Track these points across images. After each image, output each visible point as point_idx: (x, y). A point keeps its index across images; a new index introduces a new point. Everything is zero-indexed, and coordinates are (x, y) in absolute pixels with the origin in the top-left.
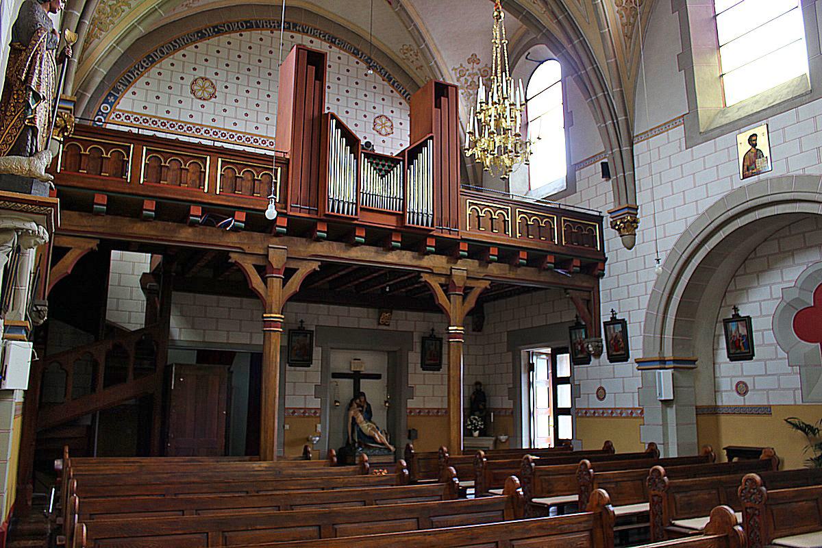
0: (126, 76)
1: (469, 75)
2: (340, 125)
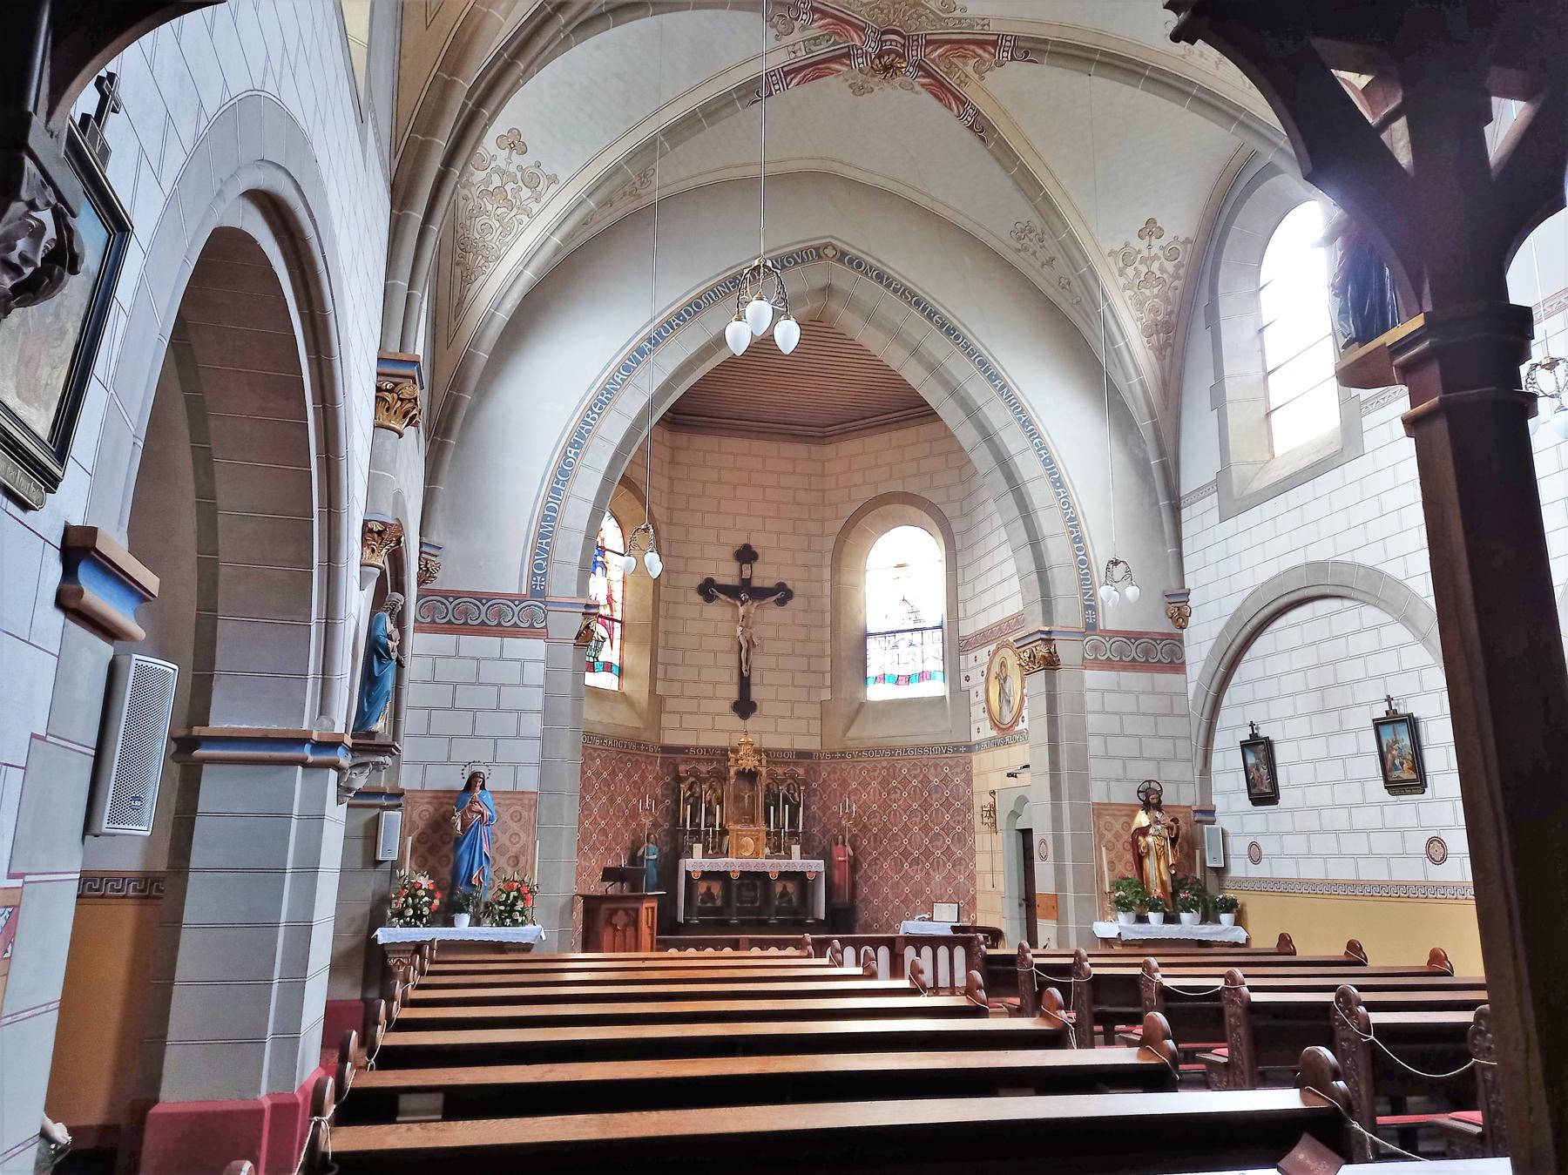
1: (1143, 261)
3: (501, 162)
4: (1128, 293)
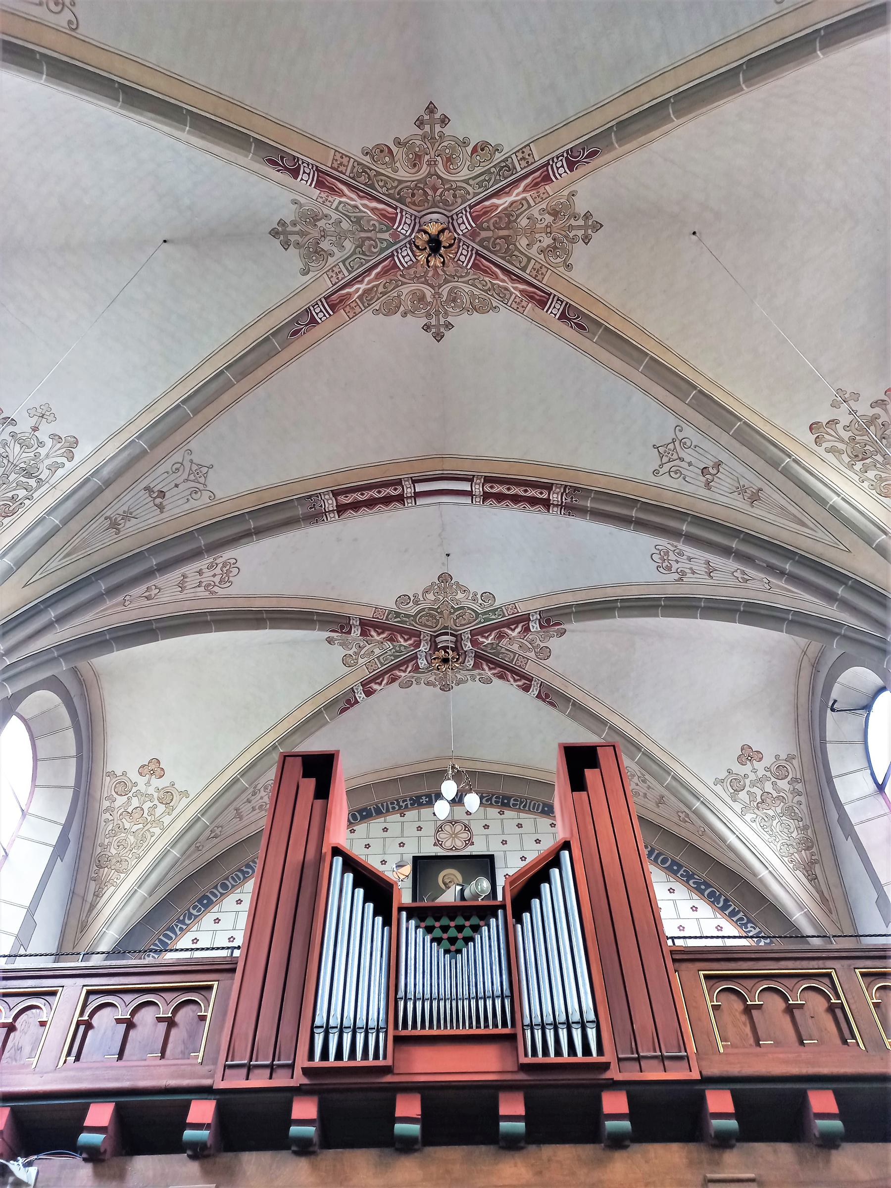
0: (161, 937)
1: (753, 785)
2: (351, 864)
3: (141, 787)
4: (748, 817)
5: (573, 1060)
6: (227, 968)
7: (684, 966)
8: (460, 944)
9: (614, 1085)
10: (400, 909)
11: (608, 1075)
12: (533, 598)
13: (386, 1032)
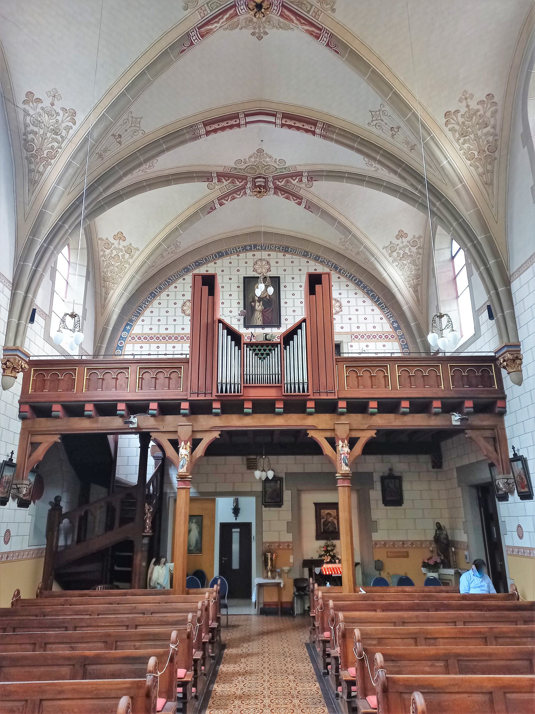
2: (226, 327)
5: (299, 394)
6: (186, 361)
7: (340, 363)
8: (265, 356)
9: (311, 400)
10: (244, 344)
11: (309, 397)
12: (305, 165)
13: (241, 385)
